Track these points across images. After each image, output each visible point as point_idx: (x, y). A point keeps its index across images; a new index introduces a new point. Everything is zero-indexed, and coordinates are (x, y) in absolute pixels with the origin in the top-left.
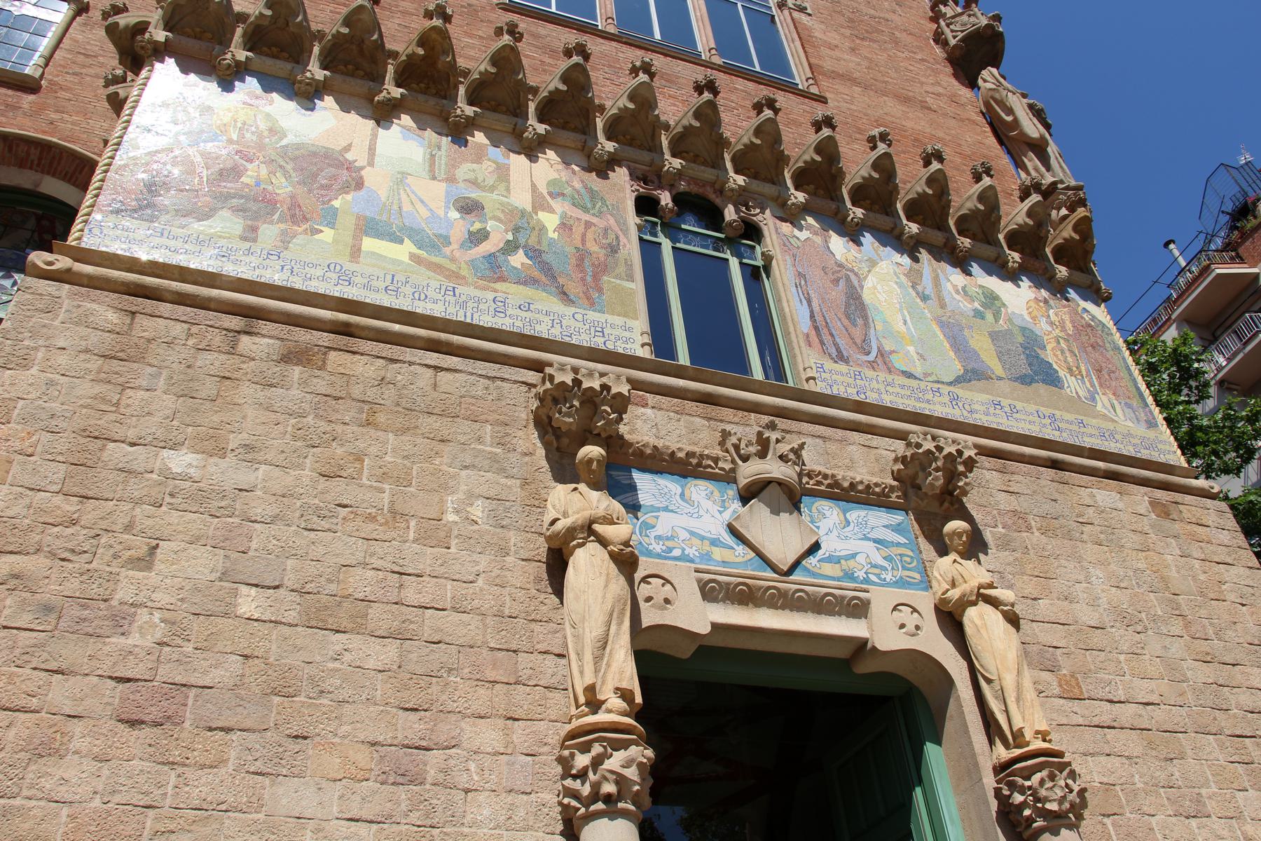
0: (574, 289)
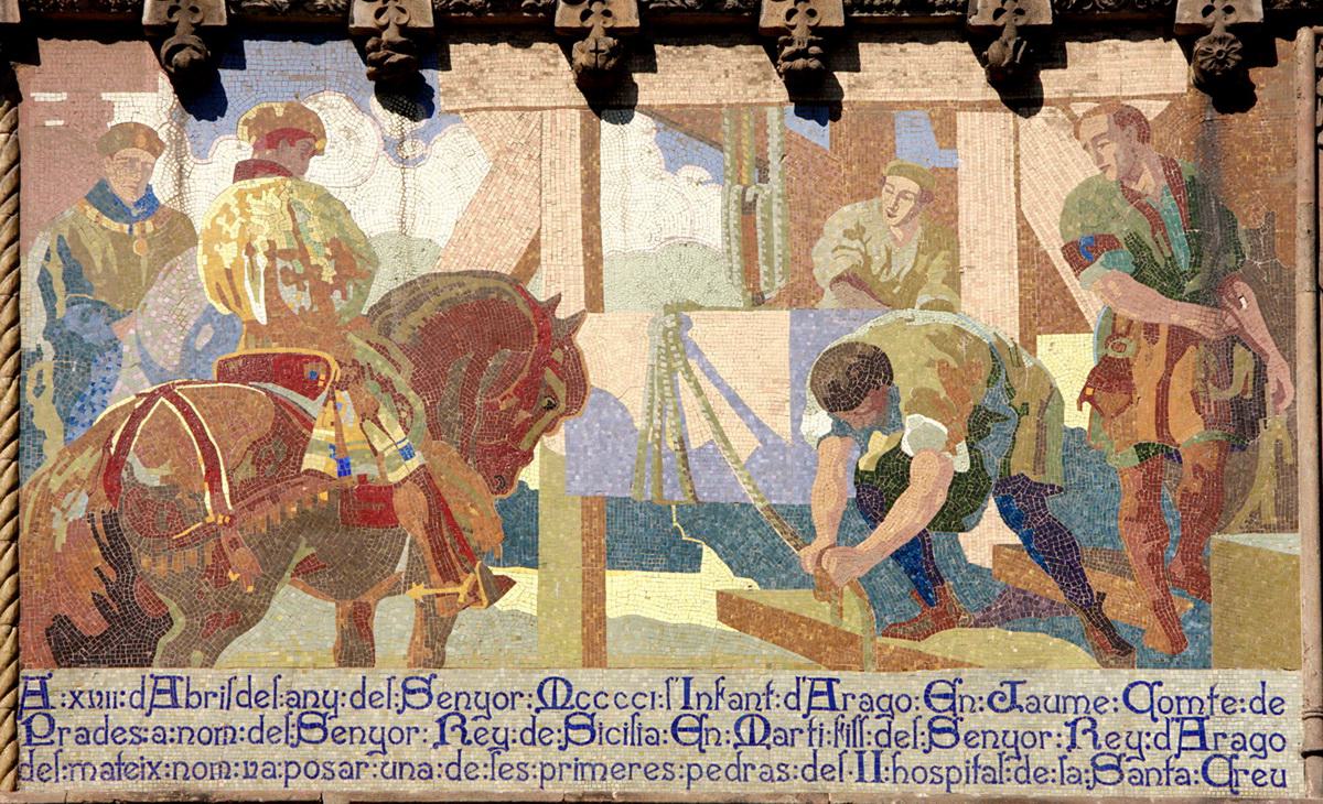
0: (1126, 601)
